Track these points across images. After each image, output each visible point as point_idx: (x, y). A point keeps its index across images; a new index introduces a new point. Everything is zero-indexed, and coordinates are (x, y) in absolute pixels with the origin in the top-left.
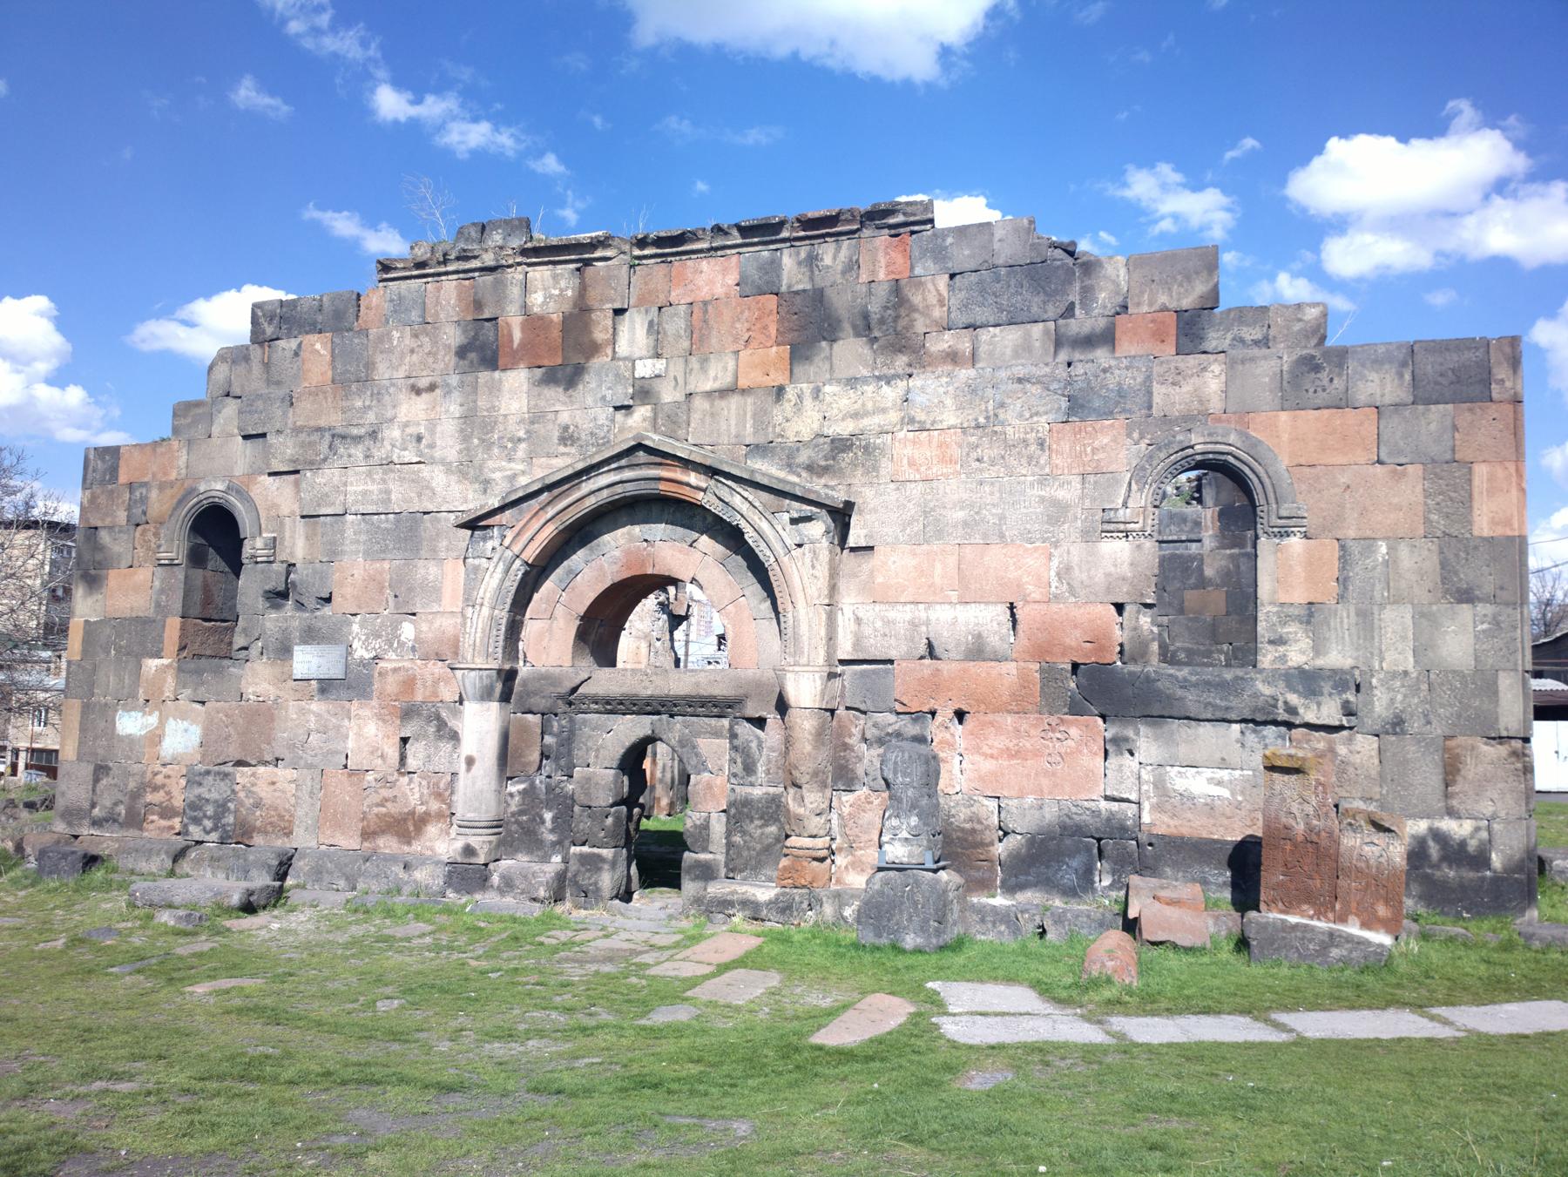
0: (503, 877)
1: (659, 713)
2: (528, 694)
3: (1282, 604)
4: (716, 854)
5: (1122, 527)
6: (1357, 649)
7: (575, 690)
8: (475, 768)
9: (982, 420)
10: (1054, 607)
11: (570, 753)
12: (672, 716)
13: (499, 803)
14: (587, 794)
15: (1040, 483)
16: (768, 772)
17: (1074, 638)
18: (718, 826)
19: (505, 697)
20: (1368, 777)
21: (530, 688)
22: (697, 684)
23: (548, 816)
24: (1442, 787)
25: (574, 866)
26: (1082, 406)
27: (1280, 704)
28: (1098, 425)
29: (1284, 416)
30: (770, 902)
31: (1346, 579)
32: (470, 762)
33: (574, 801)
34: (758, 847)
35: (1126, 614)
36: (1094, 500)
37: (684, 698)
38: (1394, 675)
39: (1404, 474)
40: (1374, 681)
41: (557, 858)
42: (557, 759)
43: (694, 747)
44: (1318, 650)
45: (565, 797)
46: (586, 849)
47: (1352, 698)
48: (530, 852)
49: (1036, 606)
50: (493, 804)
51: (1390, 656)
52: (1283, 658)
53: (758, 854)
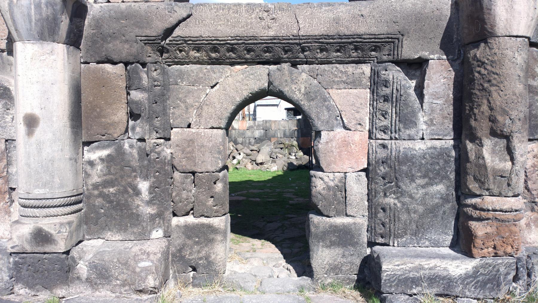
0: (93, 266)
1: (277, 62)
2: (101, 37)
4: (358, 219)
7: (169, 31)
8: (39, 131)
11: (165, 113)
12: (294, 65)
13: (76, 173)
14: (191, 158)
16: (430, 123)
18: (357, 187)
19: (74, 40)
21: (106, 29)
22: (337, 21)
23: (144, 186)
25: (178, 240)
30: (467, 276)
32: (31, 122)
33: (173, 167)
34: (421, 209)
37: (316, 39)
41: (157, 233)
42: (150, 119)
43: (325, 100)
45: (163, 162)
46: (190, 219)
48: (122, 228)
50: (69, 175)
53: (421, 216)
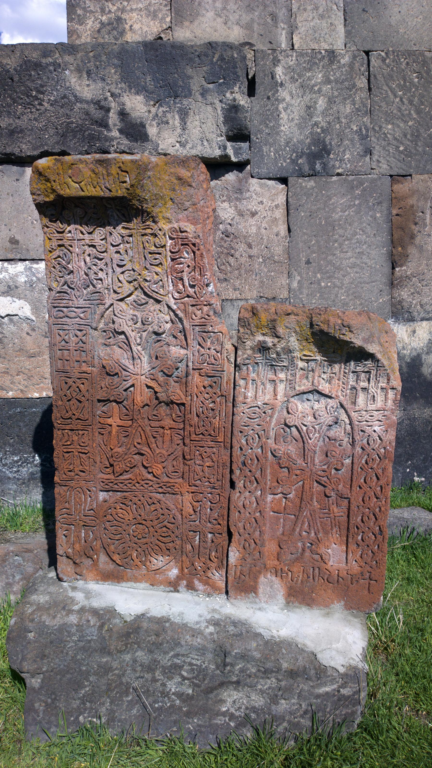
20: (269, 259)
24: (387, 269)
27: (113, 118)
38: (312, 59)
47: (243, 100)
51: (306, 22)
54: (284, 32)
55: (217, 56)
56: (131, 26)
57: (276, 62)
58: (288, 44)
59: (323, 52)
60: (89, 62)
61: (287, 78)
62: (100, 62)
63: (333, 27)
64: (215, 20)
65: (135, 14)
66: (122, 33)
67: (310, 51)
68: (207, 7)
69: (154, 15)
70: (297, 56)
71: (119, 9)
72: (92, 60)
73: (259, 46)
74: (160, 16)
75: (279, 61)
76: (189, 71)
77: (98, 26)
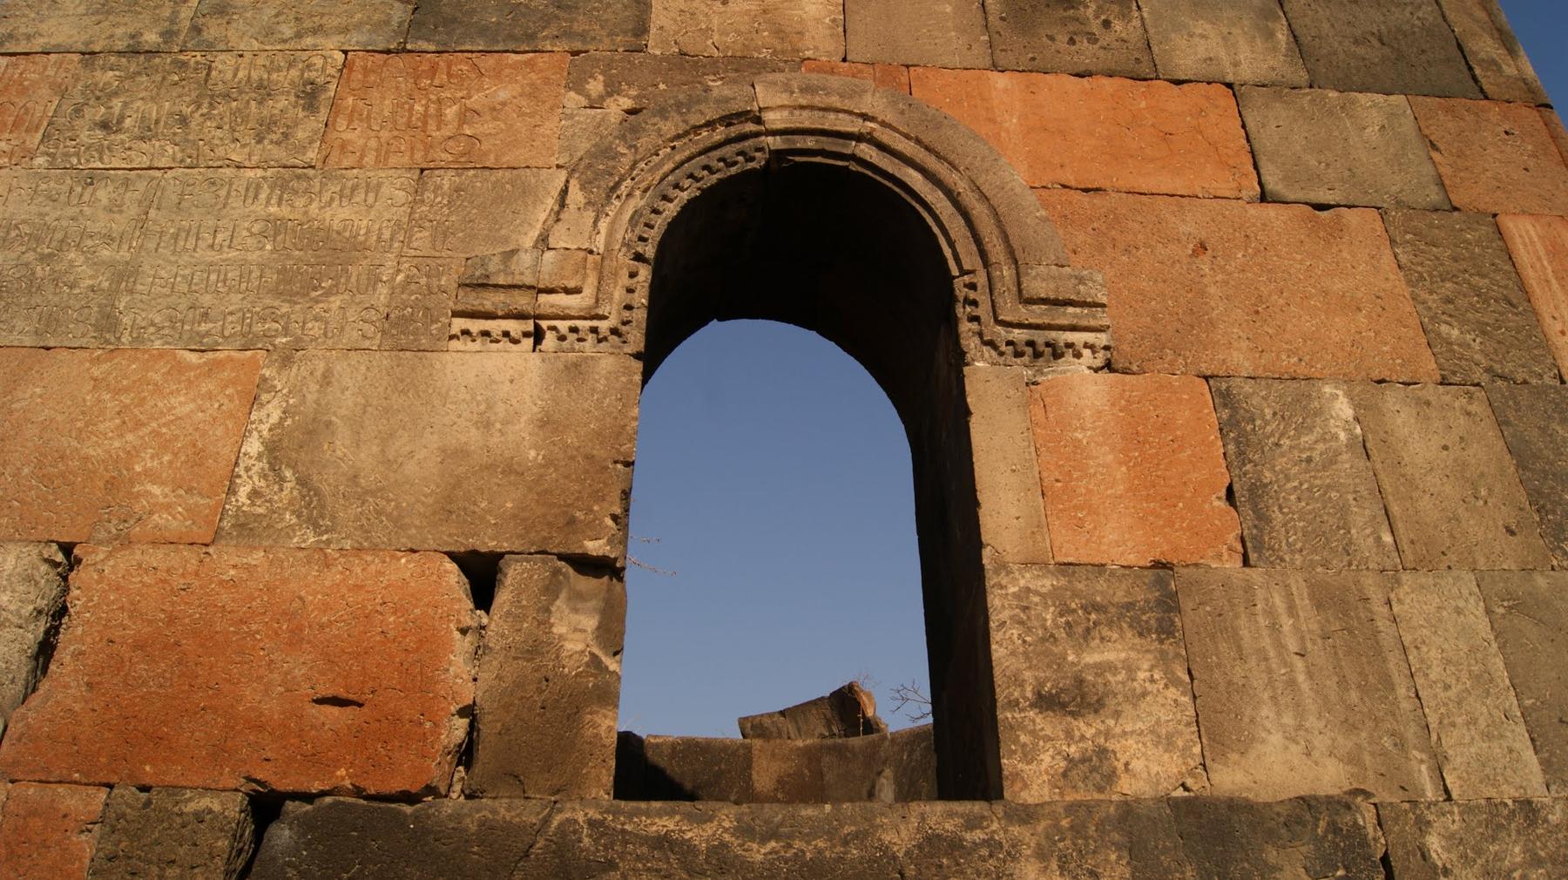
3: (1065, 567)
5: (522, 301)
6: (1350, 727)
9: (151, 38)
10: (228, 560)
15: (281, 185)
17: (274, 686)
26: (449, 22)
28: (491, 60)
29: (1001, 81)
31: (1257, 490)
35: (503, 598)
36: (442, 233)
39: (1339, 229)
40: (1434, 843)
44: (1216, 728)
49: (156, 557)
52: (1097, 765)
54: (1423, 768)
55: (1322, 824)
56: (1127, 764)
57: (1423, 825)
58: (1437, 789)
59: (1510, 802)
60: (1062, 840)
61: (1454, 857)
62: (1086, 838)
63: (1514, 755)
64: (1286, 748)
65: (1131, 742)
66: (1111, 777)
67: (1483, 802)
68: (1268, 725)
69: (1169, 745)
70: (1461, 813)
71: (1099, 732)
72: (1069, 835)
73: (1383, 796)
74: (1180, 743)
75: (1429, 823)
76: (1272, 855)
77: (1063, 764)
